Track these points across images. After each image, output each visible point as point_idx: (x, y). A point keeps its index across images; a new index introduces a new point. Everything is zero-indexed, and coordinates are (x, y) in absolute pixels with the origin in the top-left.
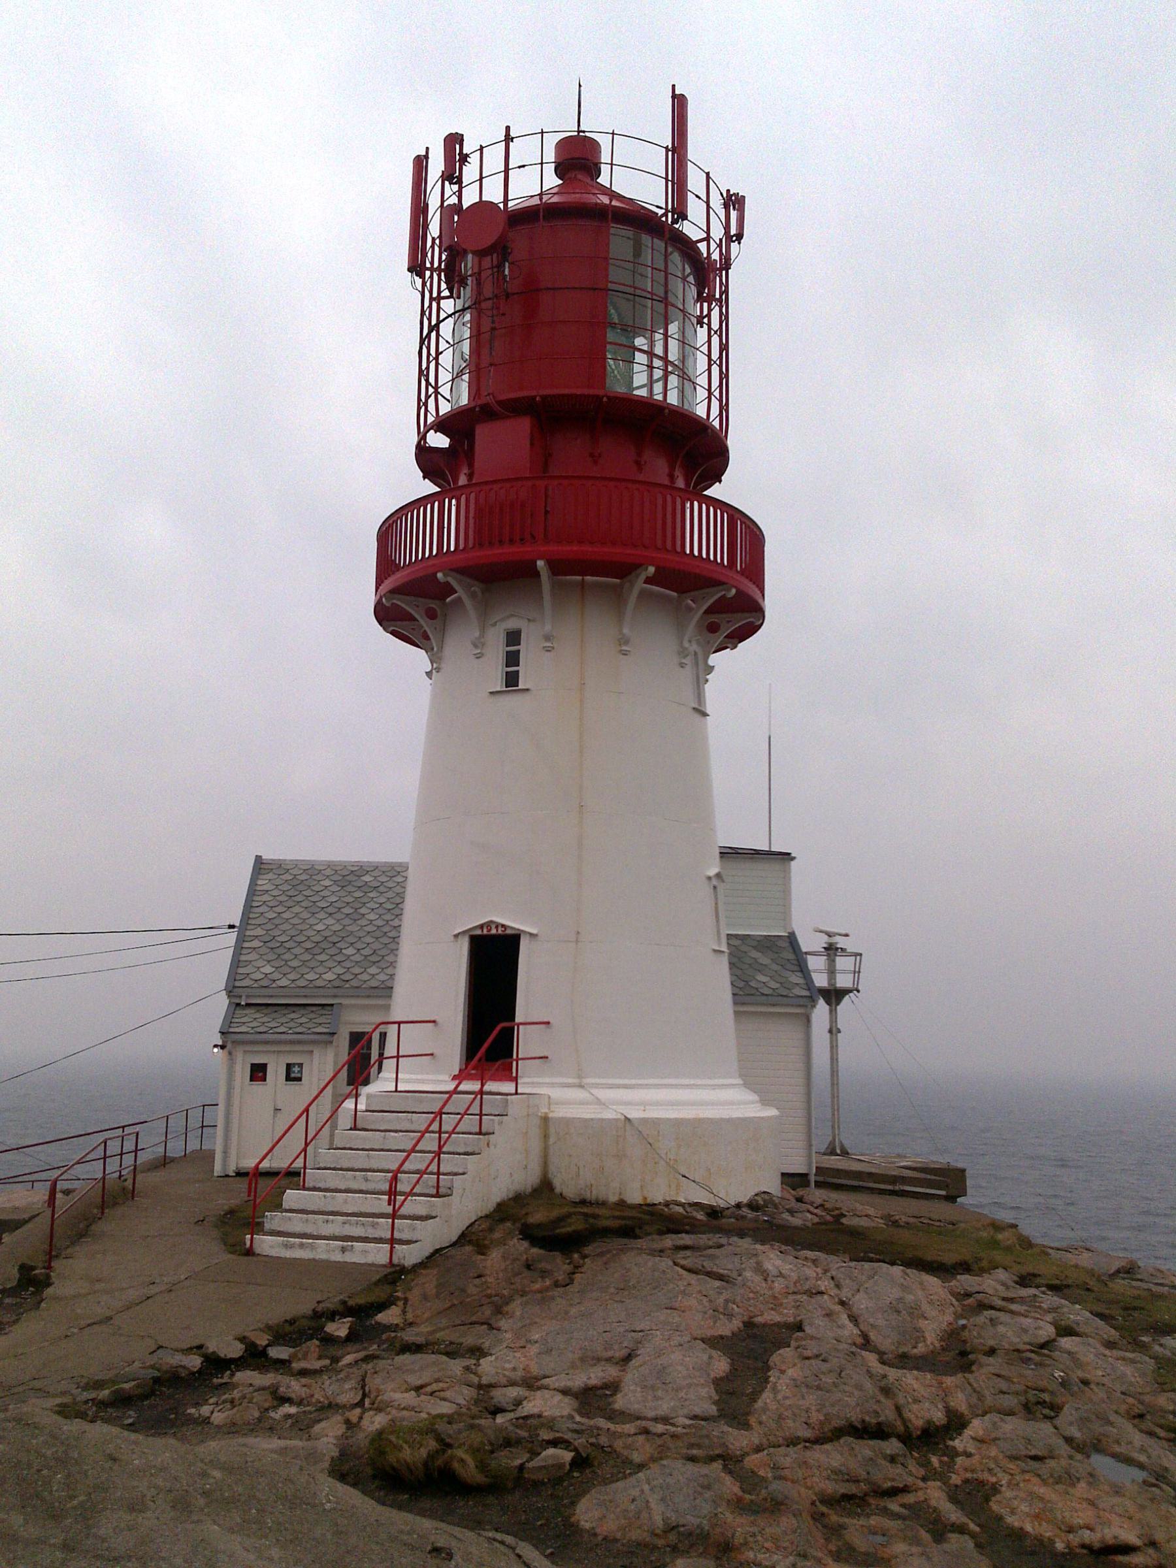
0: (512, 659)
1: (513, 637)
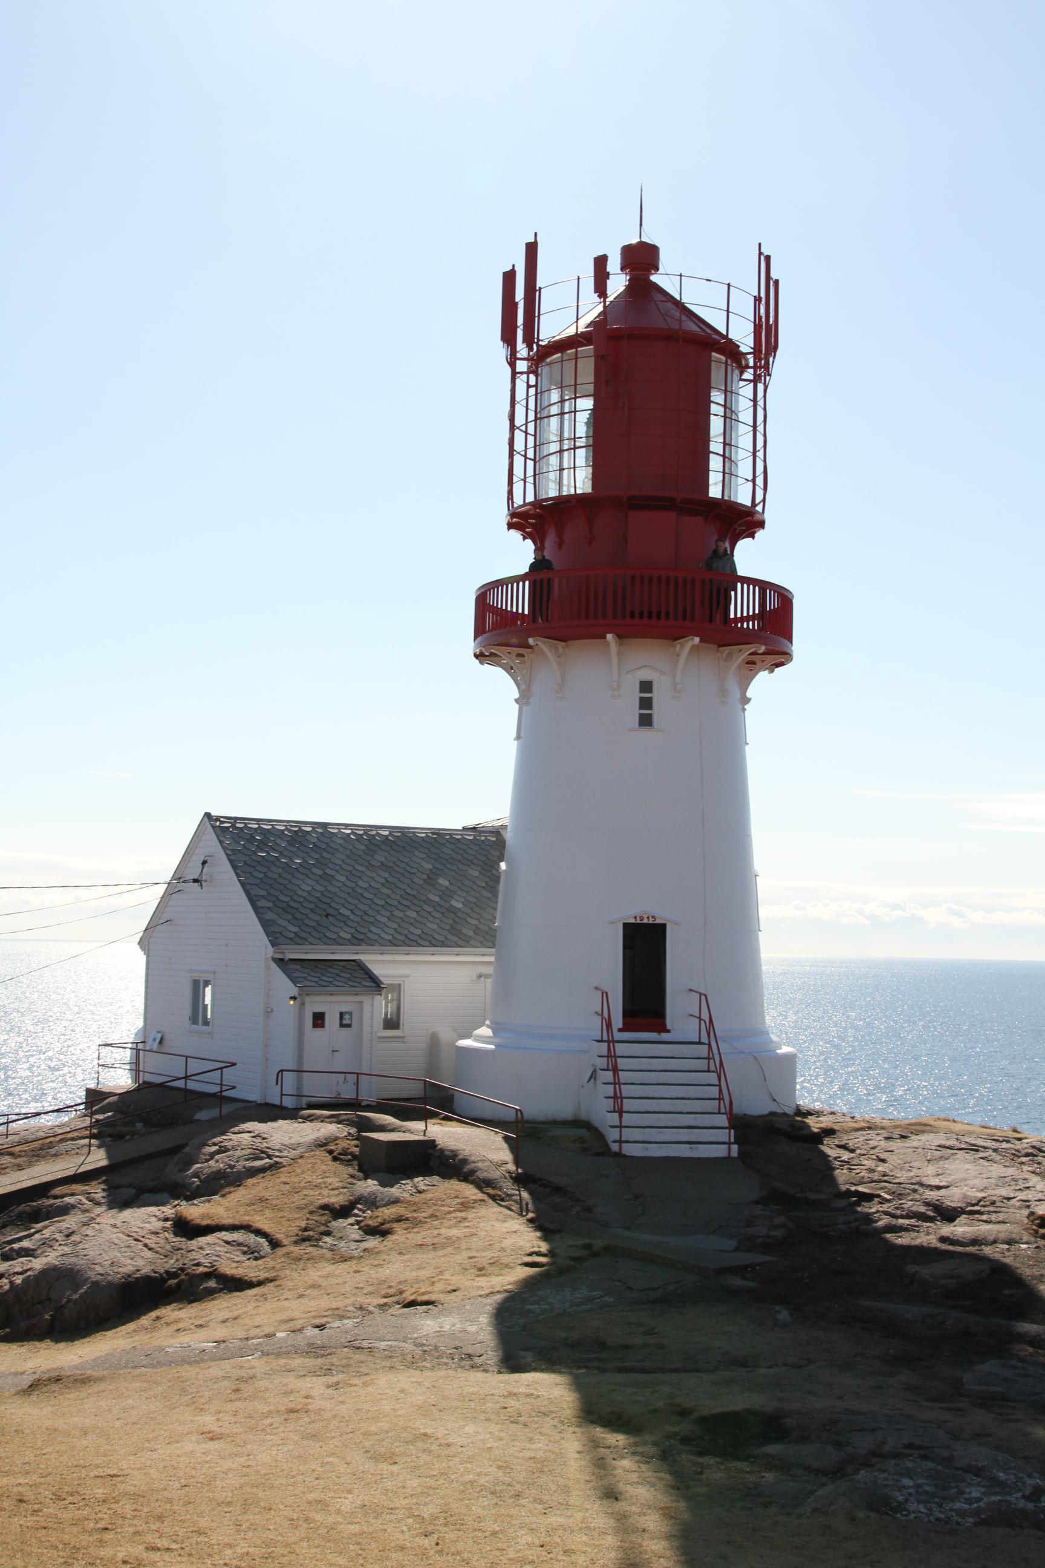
0: (646, 703)
1: (646, 686)
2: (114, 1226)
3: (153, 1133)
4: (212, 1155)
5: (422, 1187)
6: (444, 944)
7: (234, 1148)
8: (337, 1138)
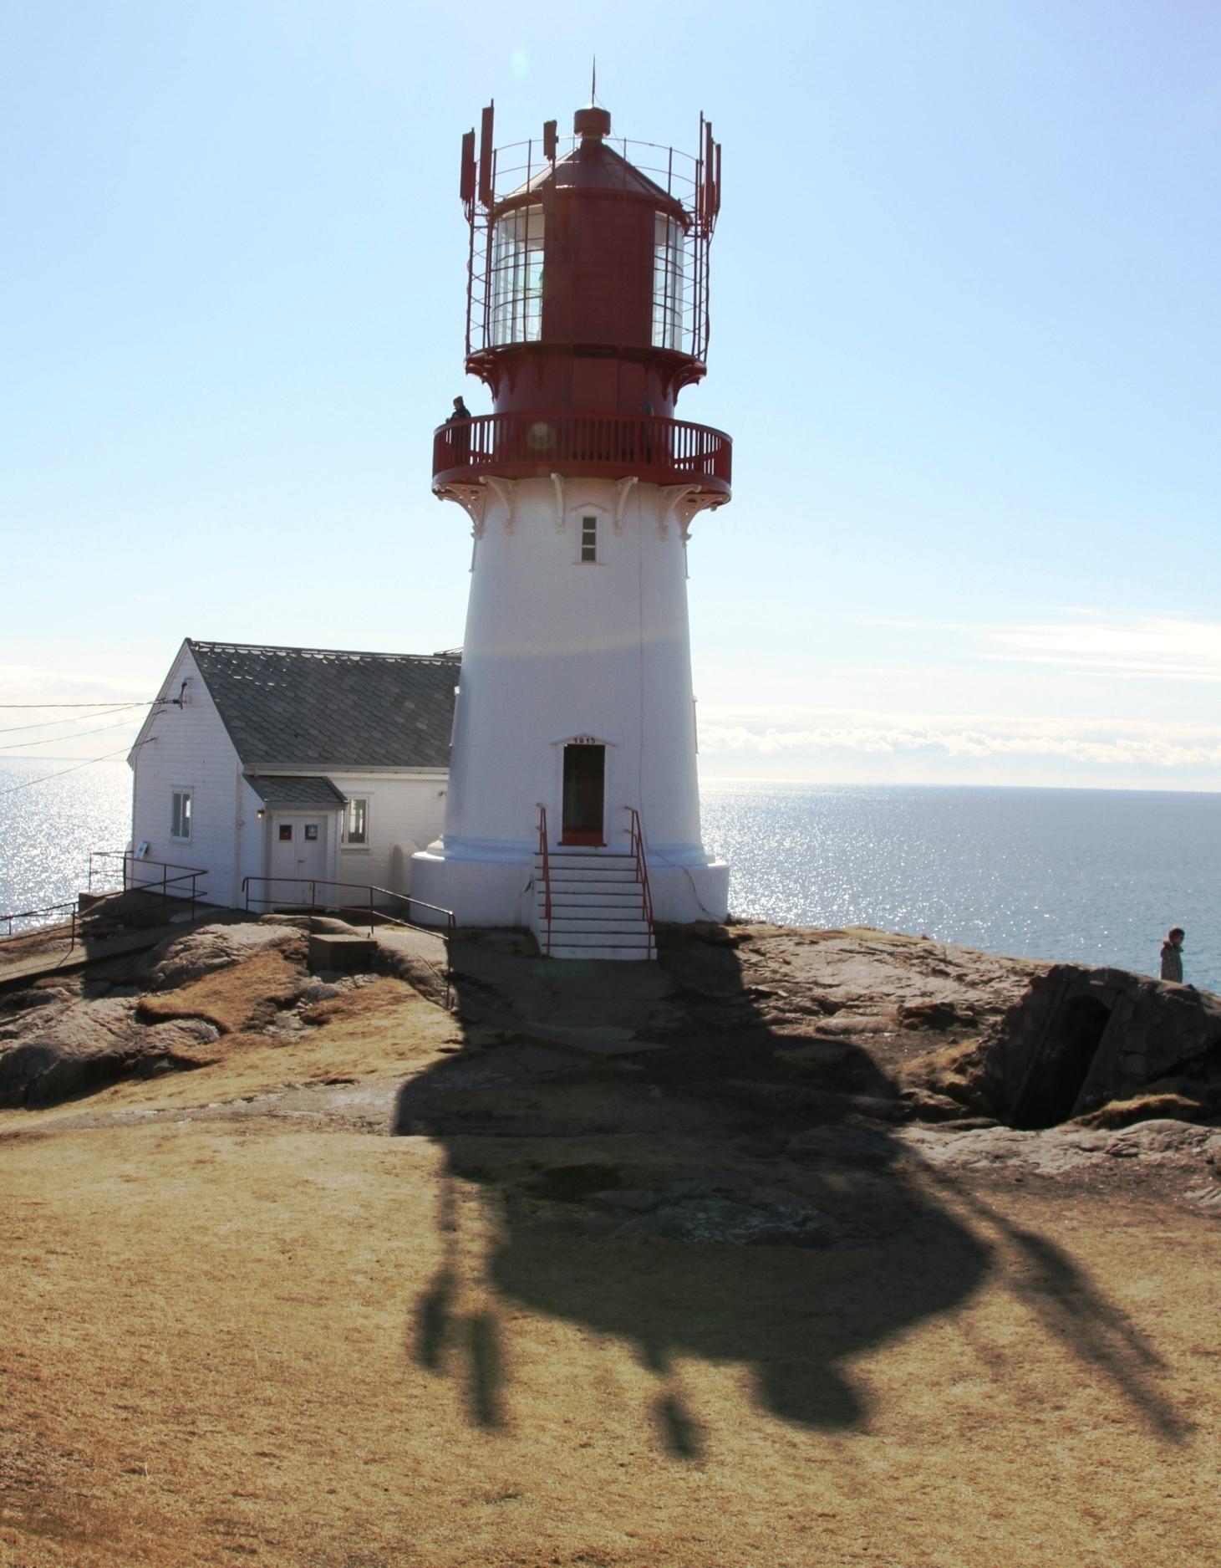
0: (589, 539)
1: (589, 523)
2: (86, 1013)
3: (129, 936)
4: (177, 953)
5: (361, 983)
6: (407, 764)
7: (197, 947)
8: (290, 939)
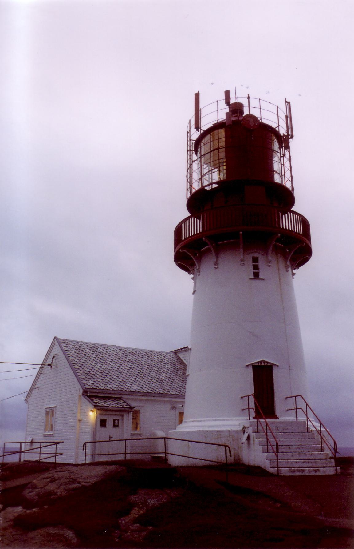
0: (256, 268)
1: (255, 260)
